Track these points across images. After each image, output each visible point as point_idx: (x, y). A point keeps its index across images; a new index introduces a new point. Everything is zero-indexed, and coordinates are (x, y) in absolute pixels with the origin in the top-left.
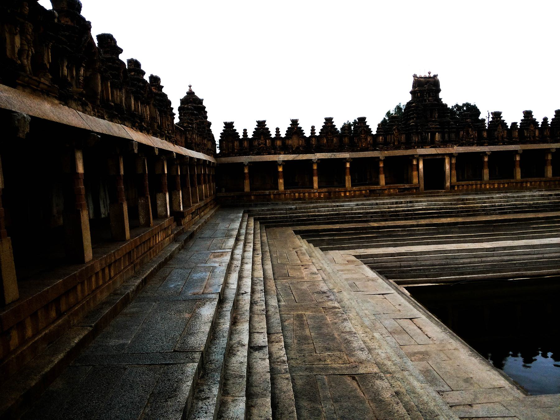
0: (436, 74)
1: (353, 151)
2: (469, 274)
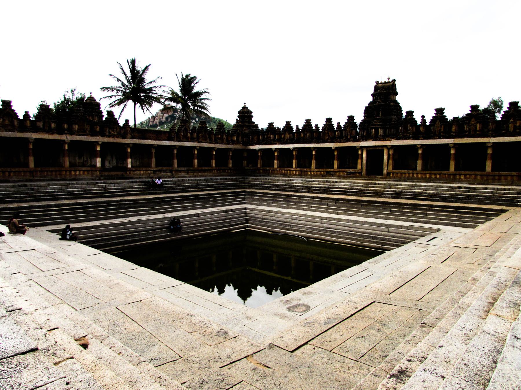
2: (292, 230)
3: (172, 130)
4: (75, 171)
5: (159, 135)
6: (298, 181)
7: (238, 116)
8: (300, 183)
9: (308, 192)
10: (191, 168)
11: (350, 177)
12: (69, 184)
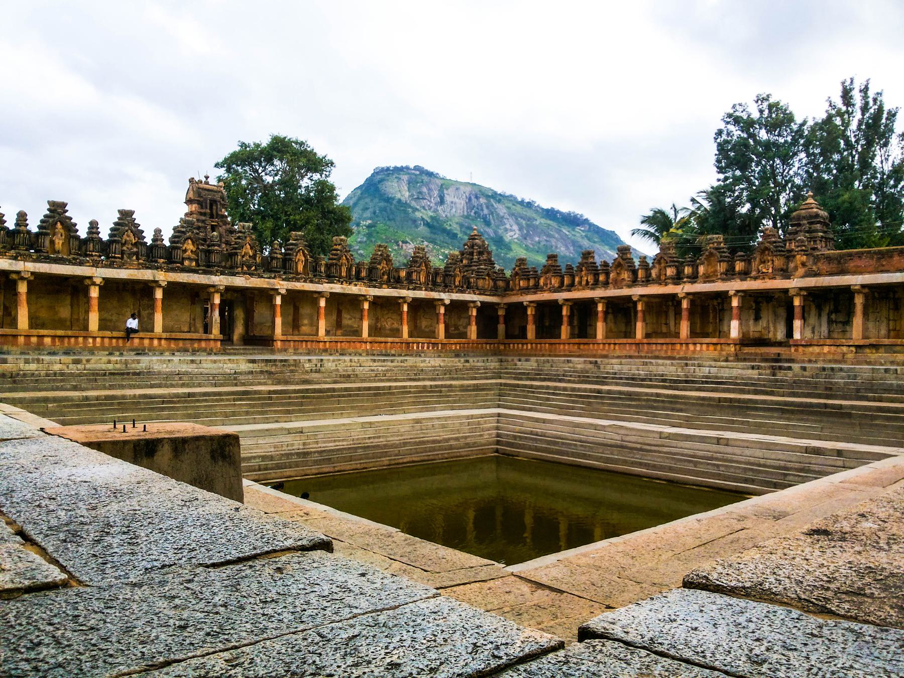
4: (695, 344)
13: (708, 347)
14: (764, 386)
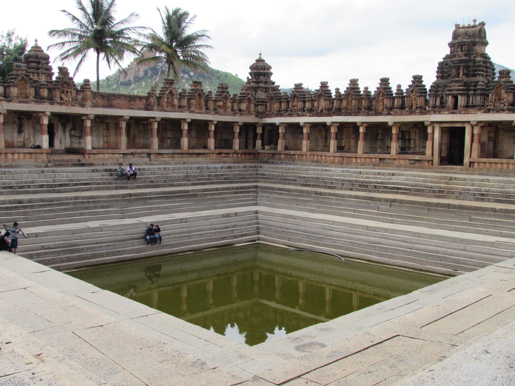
0: (481, 22)
1: (368, 115)
2: (323, 245)
3: (150, 95)
4: (13, 153)
5: (131, 100)
6: (336, 172)
7: (251, 74)
8: (340, 176)
9: (351, 190)
10: (178, 151)
11: (415, 167)
12: (5, 173)
13: (25, 156)
14: (110, 183)
